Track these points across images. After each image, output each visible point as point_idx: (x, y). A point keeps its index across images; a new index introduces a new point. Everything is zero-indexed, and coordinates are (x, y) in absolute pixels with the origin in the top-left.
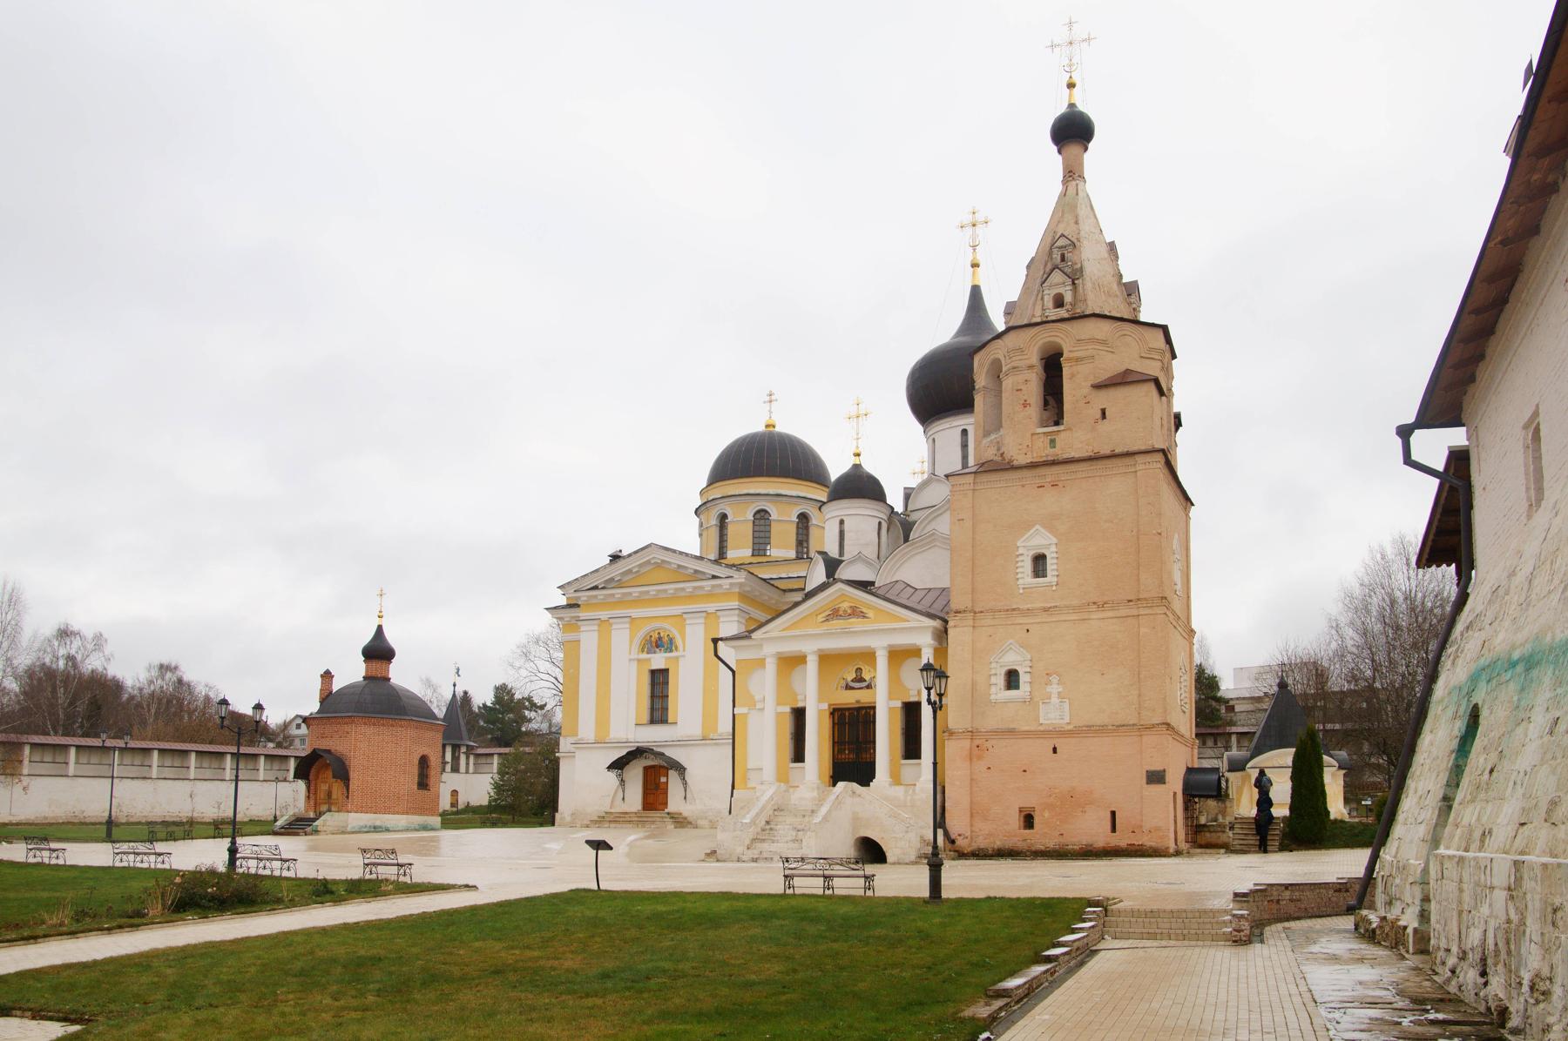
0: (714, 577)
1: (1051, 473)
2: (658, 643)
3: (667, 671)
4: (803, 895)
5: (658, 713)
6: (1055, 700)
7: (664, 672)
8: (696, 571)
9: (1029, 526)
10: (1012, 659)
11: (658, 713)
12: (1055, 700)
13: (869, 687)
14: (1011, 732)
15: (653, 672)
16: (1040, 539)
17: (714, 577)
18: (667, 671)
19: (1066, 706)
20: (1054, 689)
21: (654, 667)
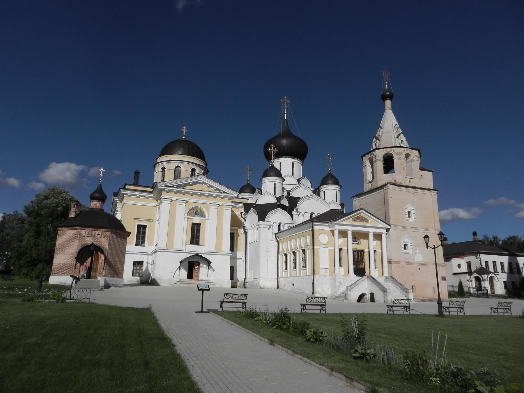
0: (224, 192)
1: (412, 190)
2: (196, 211)
3: (200, 224)
4: (470, 316)
5: (195, 239)
6: (418, 254)
7: (199, 225)
8: (217, 189)
9: (407, 204)
10: (406, 241)
11: (195, 239)
12: (418, 254)
13: (358, 244)
14: (409, 262)
15: (193, 224)
16: (409, 207)
17: (224, 192)
18: (200, 224)
19: (421, 256)
20: (418, 251)
21: (195, 222)
